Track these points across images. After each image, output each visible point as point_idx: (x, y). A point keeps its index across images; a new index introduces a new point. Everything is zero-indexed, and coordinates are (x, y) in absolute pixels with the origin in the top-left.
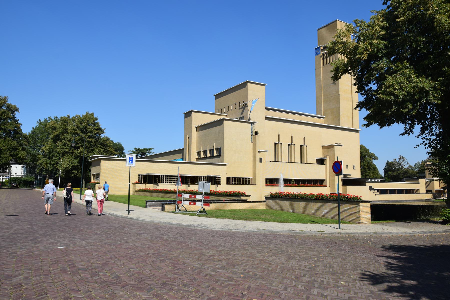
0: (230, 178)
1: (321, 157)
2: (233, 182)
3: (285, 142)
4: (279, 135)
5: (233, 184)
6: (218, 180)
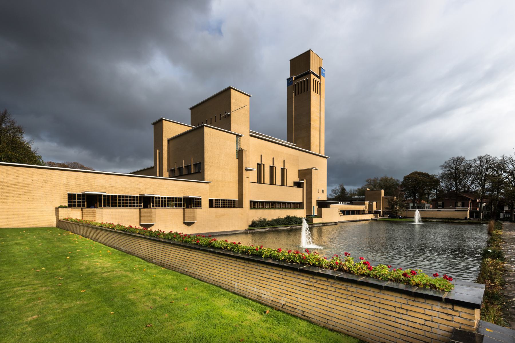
0: (212, 200)
1: (297, 179)
2: (216, 204)
3: (267, 163)
4: (261, 156)
5: (216, 207)
6: (198, 202)
